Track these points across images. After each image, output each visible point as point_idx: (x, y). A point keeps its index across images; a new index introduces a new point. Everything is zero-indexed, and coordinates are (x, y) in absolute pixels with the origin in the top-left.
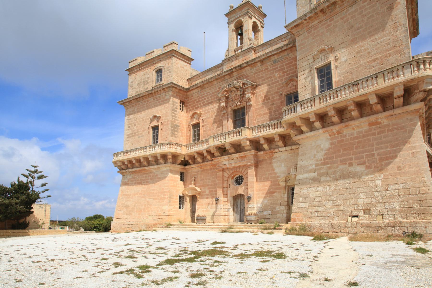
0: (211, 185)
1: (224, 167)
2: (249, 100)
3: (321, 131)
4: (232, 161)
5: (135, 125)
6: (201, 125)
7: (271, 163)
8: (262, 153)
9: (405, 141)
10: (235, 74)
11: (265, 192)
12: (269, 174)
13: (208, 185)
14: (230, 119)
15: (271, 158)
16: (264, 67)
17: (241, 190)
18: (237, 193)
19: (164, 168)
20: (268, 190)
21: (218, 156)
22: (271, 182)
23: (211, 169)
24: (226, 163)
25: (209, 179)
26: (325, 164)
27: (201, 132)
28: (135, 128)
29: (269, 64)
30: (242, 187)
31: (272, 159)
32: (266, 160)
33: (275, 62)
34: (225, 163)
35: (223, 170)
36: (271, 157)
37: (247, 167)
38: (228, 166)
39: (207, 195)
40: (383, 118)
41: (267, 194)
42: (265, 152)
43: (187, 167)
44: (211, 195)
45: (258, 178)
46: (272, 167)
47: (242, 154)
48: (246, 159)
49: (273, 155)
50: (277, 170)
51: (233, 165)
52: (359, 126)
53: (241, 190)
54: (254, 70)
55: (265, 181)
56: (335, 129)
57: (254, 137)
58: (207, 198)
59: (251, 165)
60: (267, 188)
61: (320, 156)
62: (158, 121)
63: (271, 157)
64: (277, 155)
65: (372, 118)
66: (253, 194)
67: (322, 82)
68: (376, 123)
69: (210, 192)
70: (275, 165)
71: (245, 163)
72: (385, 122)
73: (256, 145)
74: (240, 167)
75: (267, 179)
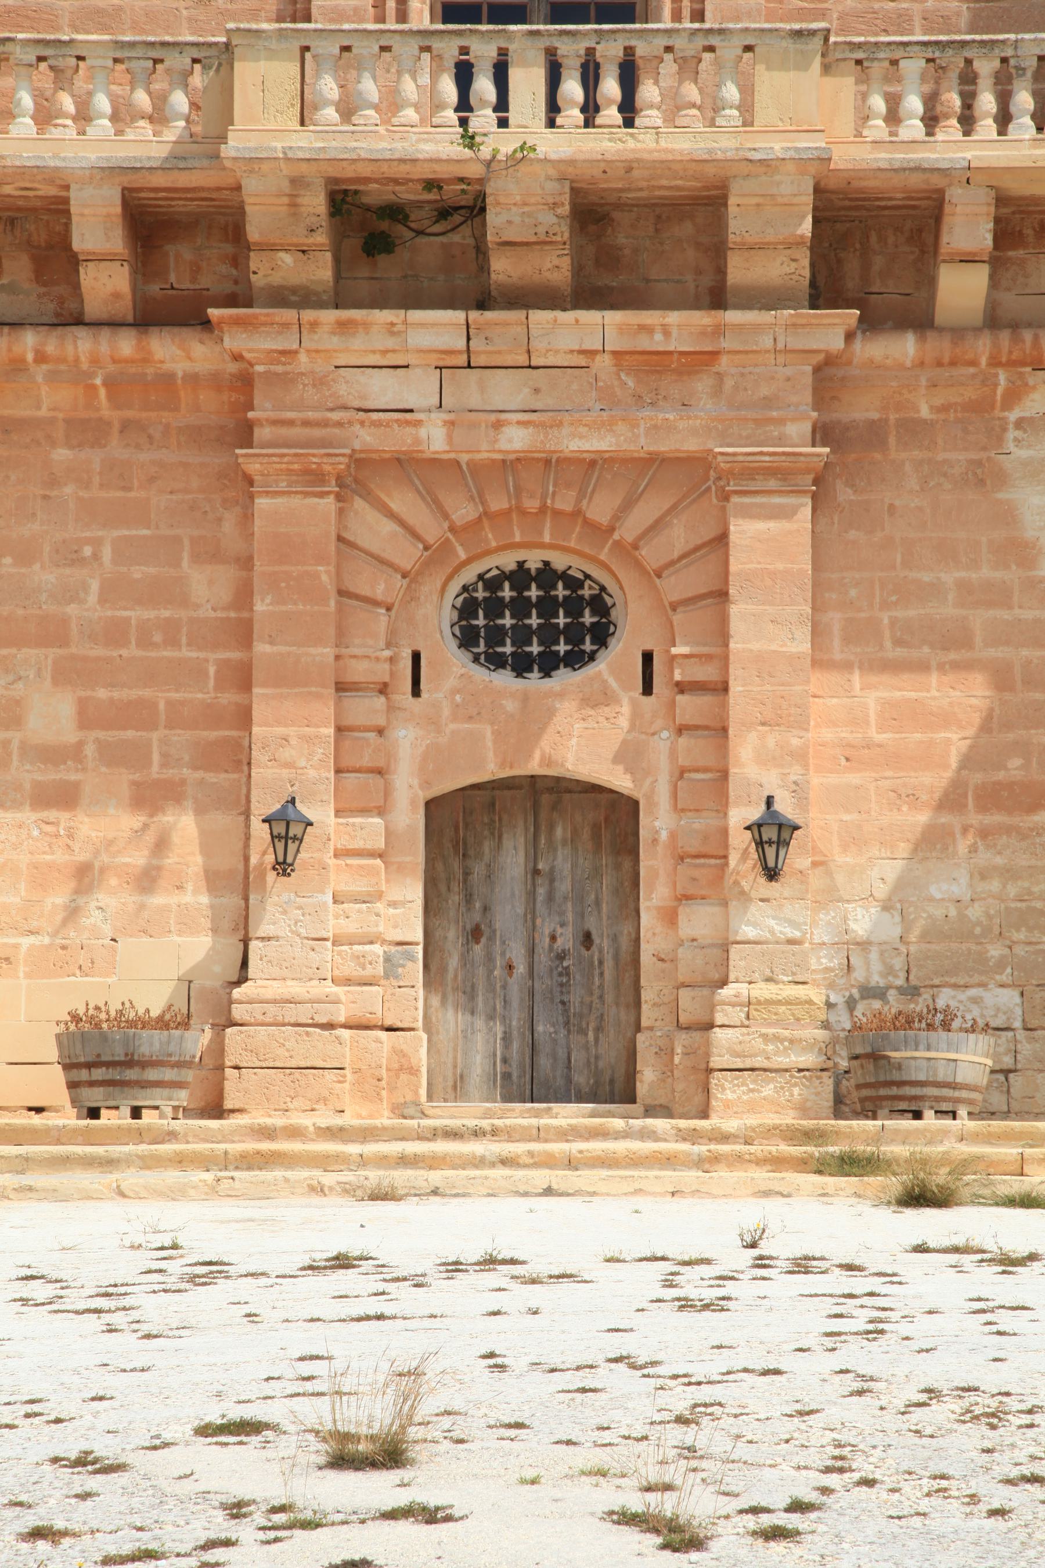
0: (115, 633)
1: (364, 438)
4: (506, 391)
7: (985, 477)
8: (905, 347)
11: (934, 781)
12: (964, 587)
13: (53, 633)
15: (982, 418)
17: (584, 729)
18: (534, 767)
20: (967, 762)
21: (298, 297)
22: (1002, 679)
23: (85, 431)
24: (417, 390)
25: (70, 556)
30: (602, 698)
31: (996, 436)
32: (913, 430)
34: (383, 389)
35: (357, 478)
36: (982, 407)
37: (706, 483)
38: (434, 437)
39: (51, 755)
41: (951, 800)
42: (938, 346)
44: (113, 756)
45: (835, 619)
46: (1008, 516)
47: (677, 328)
48: (702, 384)
49: (1013, 396)
51: (516, 439)
53: (584, 729)
55: (923, 667)
57: (883, 158)
58: (64, 797)
59: (782, 474)
60: (956, 742)
63: (982, 407)
66: (799, 790)
69: (86, 718)
71: (682, 427)
74: (591, 465)
75: (946, 646)
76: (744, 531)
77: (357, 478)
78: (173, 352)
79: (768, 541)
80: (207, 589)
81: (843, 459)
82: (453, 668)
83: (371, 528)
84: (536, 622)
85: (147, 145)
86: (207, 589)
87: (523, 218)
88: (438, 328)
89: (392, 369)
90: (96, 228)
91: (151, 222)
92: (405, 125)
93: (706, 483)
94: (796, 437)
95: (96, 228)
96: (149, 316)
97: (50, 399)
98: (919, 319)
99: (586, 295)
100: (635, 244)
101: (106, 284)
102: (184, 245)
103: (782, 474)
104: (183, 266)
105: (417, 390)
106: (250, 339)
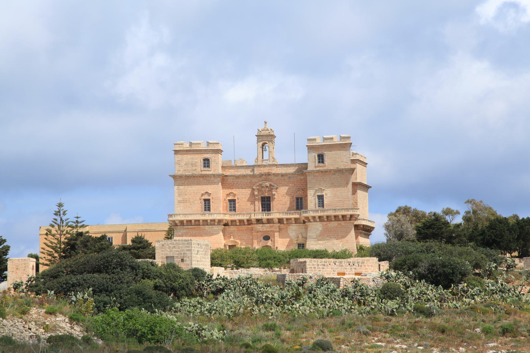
2: (275, 195)
3: (319, 223)
5: (186, 195)
6: (237, 201)
7: (287, 231)
9: (349, 232)
10: (264, 177)
14: (256, 203)
15: (287, 228)
16: (283, 178)
17: (269, 243)
19: (216, 228)
23: (245, 230)
24: (260, 228)
26: (320, 236)
27: (237, 205)
28: (186, 197)
29: (286, 177)
33: (290, 177)
35: (258, 232)
37: (274, 232)
40: (343, 223)
43: (226, 227)
47: (272, 225)
50: (291, 235)
52: (334, 224)
54: (276, 178)
56: (325, 223)
61: (318, 232)
62: (209, 196)
64: (291, 227)
65: (339, 222)
67: (319, 201)
68: (340, 224)
70: (289, 232)
71: (273, 229)
72: (343, 224)
73: (280, 221)
76: (276, 234)
77: (258, 232)
78: (249, 226)
79: (277, 234)
80: (251, 237)
81: (280, 230)
82: (263, 240)
83: (259, 234)
84: (267, 238)
85: (248, 218)
86: (251, 237)
87: (265, 221)
88: (261, 225)
89: (259, 227)
90: (245, 221)
91: (248, 220)
92: (259, 217)
93: (274, 232)
94: (278, 230)
95: (245, 221)
96: (249, 224)
97: (244, 229)
98: (283, 223)
99: (268, 223)
100: (269, 221)
101: (246, 223)
102: (249, 222)
103: (277, 231)
104: (250, 222)
105: (260, 228)
106: (253, 226)
